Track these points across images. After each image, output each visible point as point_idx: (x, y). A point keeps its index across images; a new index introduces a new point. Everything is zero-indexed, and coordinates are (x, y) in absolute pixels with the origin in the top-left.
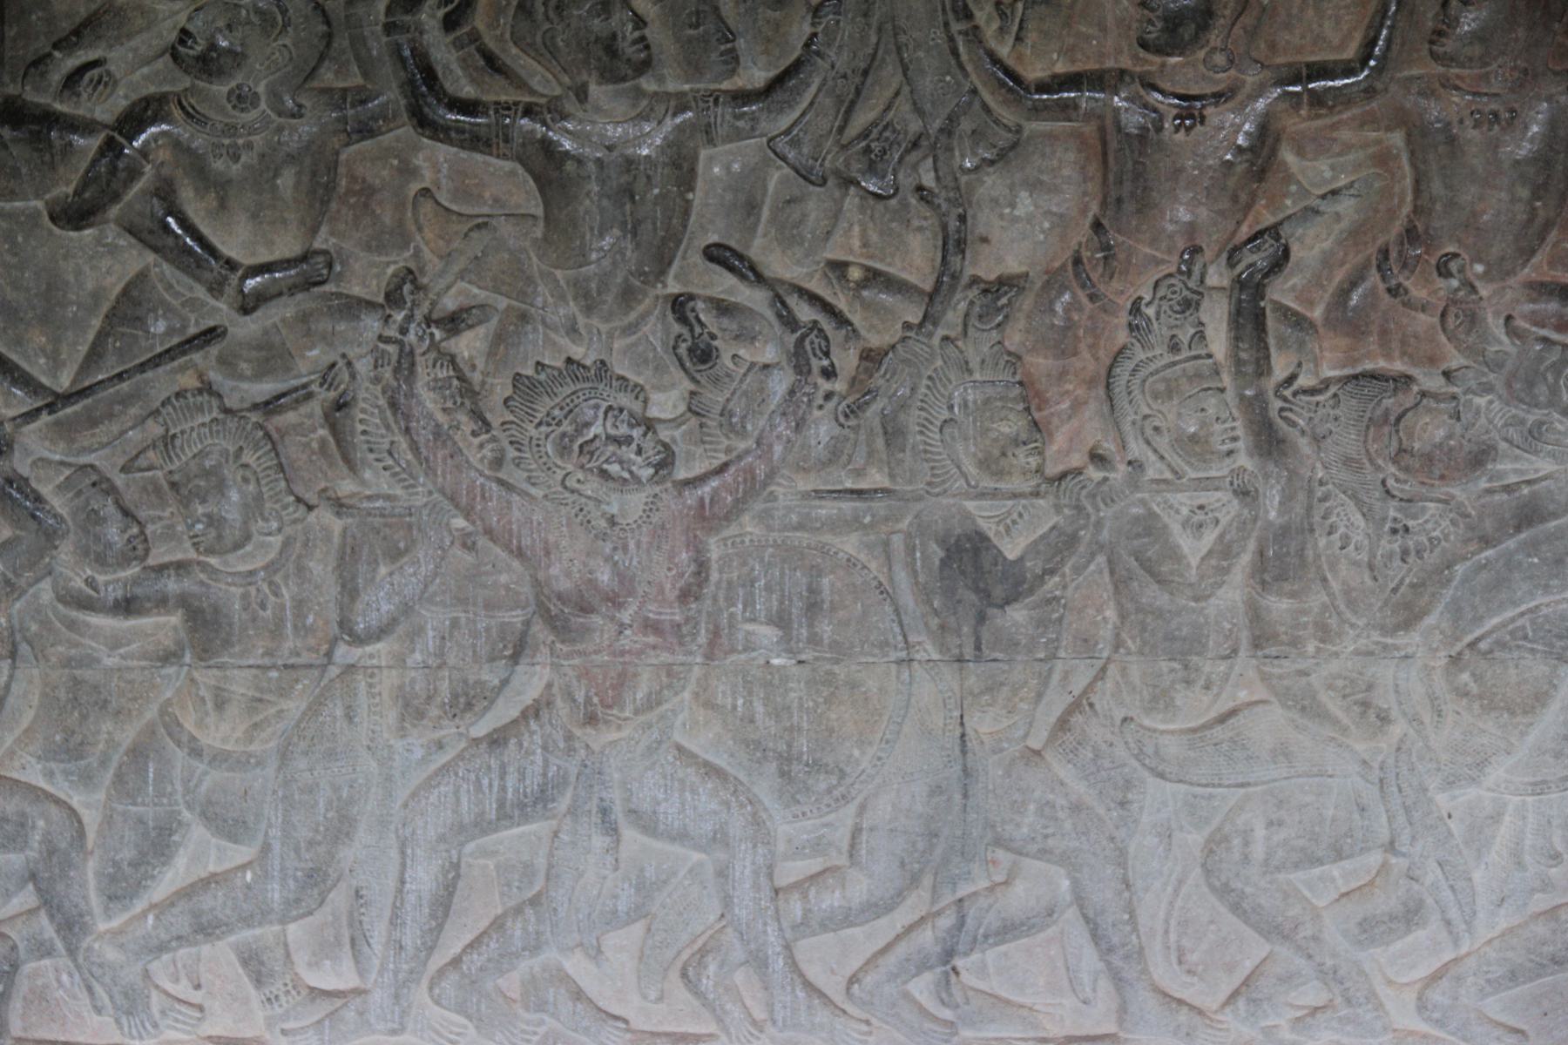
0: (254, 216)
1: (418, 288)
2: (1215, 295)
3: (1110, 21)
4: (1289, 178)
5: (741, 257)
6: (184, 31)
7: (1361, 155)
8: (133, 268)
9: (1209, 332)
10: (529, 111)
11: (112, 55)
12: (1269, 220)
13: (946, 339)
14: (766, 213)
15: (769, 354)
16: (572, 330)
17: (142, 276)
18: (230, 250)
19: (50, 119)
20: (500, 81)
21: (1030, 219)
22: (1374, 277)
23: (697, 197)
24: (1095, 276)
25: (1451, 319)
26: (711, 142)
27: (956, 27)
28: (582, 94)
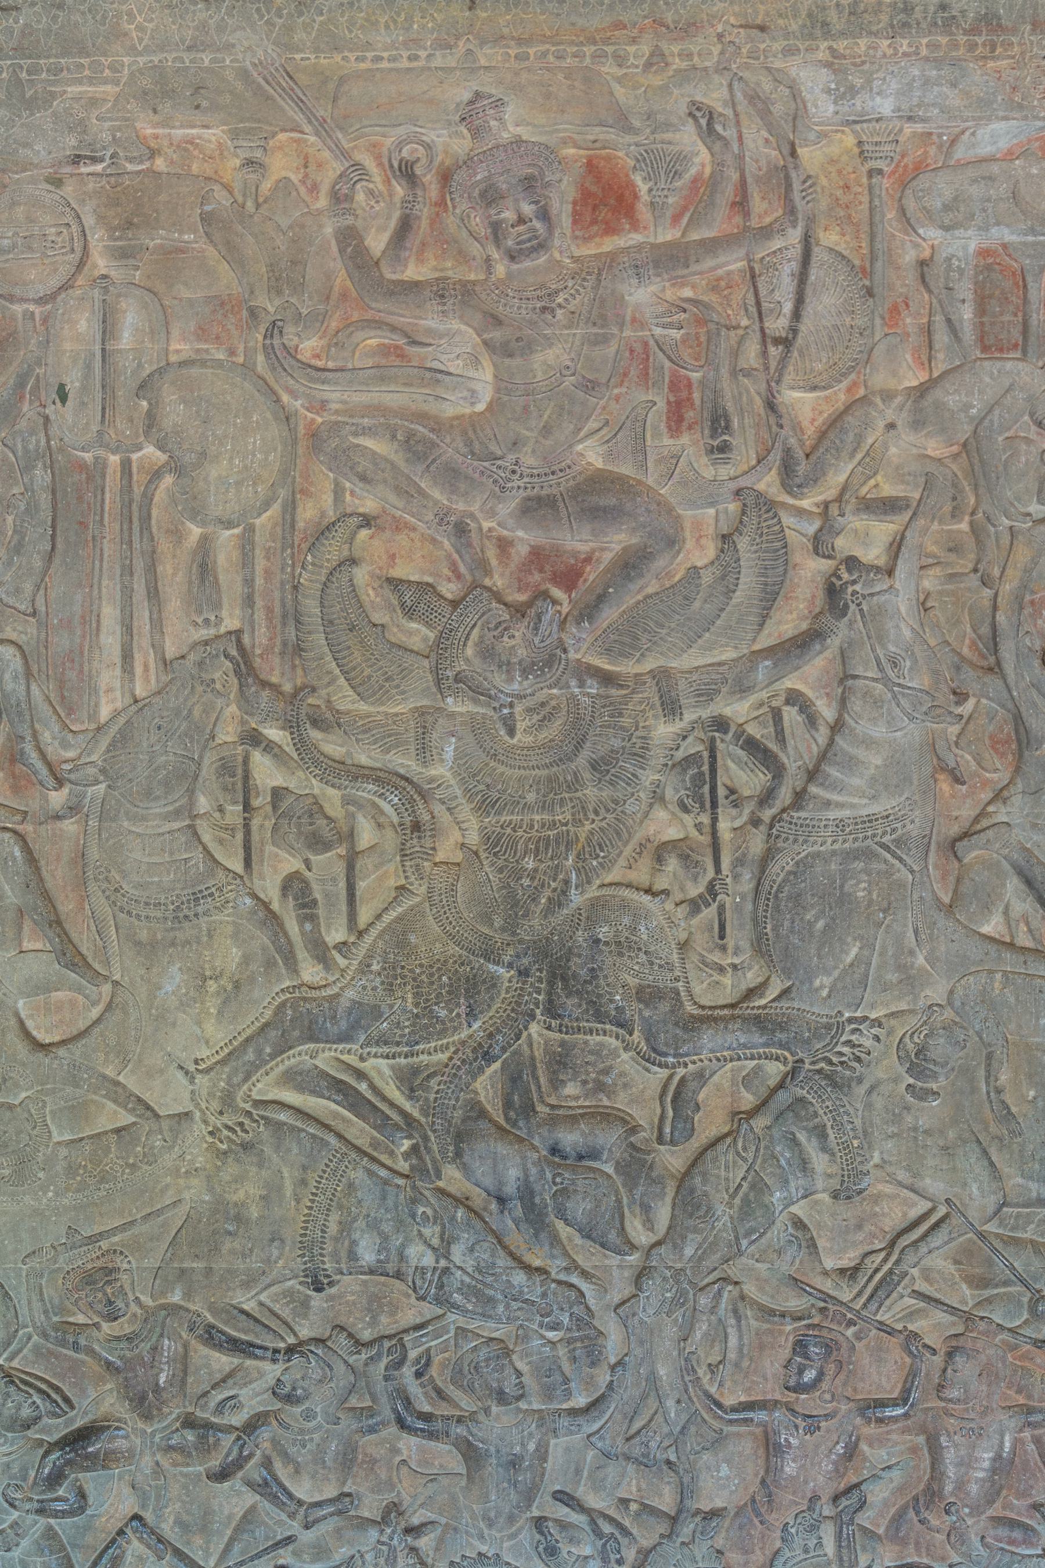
0: (313, 1477)
1: (401, 1514)
2: (828, 1522)
3: (769, 1376)
4: (865, 1459)
5: (573, 1498)
6: (279, 1380)
7: (903, 1447)
8: (249, 1503)
9: (825, 1541)
10: (460, 1420)
11: (243, 1392)
12: (855, 1480)
13: (683, 1543)
14: (585, 1473)
15: (588, 1551)
16: (481, 1537)
17: (253, 1508)
18: (299, 1494)
19: (208, 1426)
20: (444, 1404)
21: (728, 1478)
22: (911, 1514)
23: (548, 1466)
24: (763, 1510)
25: (952, 1538)
26: (556, 1437)
27: (687, 1378)
28: (487, 1411)
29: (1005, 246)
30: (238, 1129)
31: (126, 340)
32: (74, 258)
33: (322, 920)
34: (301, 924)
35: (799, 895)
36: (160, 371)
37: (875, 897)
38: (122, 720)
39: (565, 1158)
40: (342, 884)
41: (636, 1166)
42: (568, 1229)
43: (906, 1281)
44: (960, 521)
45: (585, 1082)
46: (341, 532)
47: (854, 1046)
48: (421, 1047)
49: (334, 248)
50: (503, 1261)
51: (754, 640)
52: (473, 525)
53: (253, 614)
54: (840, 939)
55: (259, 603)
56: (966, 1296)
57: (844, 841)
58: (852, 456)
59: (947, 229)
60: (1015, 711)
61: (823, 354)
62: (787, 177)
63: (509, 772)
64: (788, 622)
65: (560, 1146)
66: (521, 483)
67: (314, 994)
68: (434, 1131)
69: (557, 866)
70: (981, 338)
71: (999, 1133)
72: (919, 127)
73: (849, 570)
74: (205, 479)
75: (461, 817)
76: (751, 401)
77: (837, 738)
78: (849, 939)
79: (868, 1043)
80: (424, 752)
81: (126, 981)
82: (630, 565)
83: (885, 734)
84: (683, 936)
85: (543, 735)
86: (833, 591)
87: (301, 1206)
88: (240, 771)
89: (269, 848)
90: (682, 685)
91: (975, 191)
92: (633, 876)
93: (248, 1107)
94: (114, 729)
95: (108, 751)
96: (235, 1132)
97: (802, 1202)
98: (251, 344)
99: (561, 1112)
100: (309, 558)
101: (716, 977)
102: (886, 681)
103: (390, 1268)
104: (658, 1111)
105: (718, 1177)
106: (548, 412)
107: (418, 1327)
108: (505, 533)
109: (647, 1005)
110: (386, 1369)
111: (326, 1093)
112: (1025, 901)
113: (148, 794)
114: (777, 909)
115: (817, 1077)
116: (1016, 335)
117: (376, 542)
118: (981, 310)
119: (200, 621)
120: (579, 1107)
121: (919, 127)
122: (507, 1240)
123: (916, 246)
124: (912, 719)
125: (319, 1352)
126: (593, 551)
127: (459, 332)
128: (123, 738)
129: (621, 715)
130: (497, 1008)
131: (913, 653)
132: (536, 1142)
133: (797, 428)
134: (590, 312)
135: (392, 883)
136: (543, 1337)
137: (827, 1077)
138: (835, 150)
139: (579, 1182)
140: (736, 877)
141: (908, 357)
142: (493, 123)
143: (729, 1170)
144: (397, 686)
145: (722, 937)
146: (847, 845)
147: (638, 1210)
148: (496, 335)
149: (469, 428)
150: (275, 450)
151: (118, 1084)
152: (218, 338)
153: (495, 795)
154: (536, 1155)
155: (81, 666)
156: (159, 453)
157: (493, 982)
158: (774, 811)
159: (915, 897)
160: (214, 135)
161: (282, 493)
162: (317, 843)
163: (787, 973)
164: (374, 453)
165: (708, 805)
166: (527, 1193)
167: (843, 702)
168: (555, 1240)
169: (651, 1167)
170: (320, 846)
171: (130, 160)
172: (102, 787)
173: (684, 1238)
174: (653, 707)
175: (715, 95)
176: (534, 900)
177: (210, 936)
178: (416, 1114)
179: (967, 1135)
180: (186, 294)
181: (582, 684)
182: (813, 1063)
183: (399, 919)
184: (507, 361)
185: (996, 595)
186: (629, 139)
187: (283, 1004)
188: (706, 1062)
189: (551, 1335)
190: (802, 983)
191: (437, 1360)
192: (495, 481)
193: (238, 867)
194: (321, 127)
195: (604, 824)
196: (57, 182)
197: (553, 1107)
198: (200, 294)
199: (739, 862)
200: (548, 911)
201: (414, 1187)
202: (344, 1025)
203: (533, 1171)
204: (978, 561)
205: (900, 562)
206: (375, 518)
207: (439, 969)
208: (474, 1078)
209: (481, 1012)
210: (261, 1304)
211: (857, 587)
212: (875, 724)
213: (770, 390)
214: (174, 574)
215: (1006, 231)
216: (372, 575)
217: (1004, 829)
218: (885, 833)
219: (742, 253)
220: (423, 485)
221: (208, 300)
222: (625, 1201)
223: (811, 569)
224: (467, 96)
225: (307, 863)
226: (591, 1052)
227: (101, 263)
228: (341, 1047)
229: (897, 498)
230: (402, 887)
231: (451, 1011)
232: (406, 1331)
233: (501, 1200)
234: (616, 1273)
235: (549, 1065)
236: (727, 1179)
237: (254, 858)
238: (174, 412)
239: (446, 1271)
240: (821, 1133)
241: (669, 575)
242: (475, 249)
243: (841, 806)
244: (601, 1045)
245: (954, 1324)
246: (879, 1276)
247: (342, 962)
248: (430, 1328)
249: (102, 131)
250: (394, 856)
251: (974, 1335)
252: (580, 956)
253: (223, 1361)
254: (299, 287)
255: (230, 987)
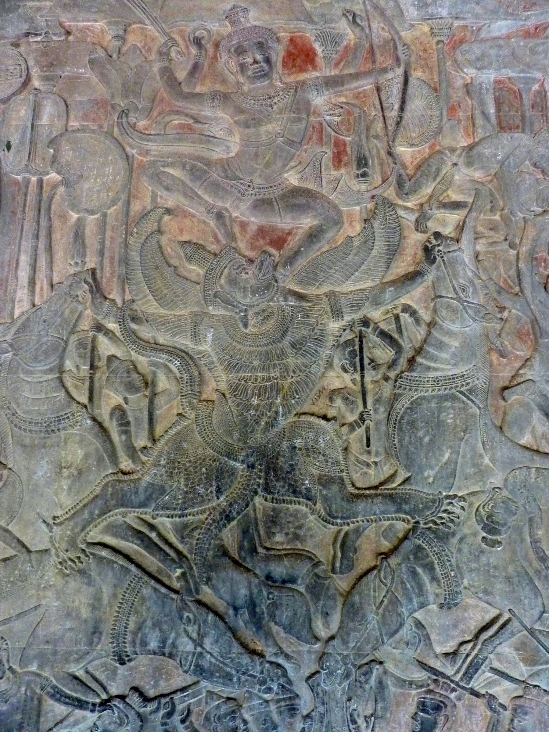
27: (352, 727)
29: (509, 78)
30: (77, 561)
31: (45, 120)
32: (22, 80)
33: (133, 434)
34: (120, 436)
35: (414, 421)
36: (61, 135)
37: (458, 422)
38: (24, 317)
39: (275, 582)
40: (146, 413)
41: (317, 588)
42: (277, 627)
43: (487, 662)
44: (495, 215)
45: (287, 534)
46: (154, 217)
47: (449, 513)
48: (189, 511)
49: (158, 77)
50: (236, 649)
51: (383, 277)
52: (226, 214)
53: (102, 260)
54: (439, 448)
55: (107, 254)
56: (521, 671)
57: (439, 390)
58: (435, 179)
59: (479, 69)
60: (532, 317)
61: (416, 129)
62: (395, 44)
63: (243, 348)
64: (402, 266)
65: (272, 575)
66: (253, 192)
67: (126, 478)
68: (196, 564)
69: (271, 404)
70: (499, 123)
71: (539, 568)
72: (461, 23)
73: (436, 239)
74: (81, 189)
75: (216, 374)
76: (378, 152)
77: (433, 331)
78: (444, 448)
79: (458, 511)
80: (196, 336)
81: (15, 469)
82: (313, 236)
83: (460, 329)
84: (345, 445)
85: (263, 328)
86: (427, 250)
87: (113, 610)
88: (89, 347)
89: (106, 391)
90: (343, 301)
91: (493, 52)
92: (315, 409)
93: (83, 546)
94: (20, 322)
95: (15, 334)
96: (74, 562)
97: (421, 611)
98: (111, 122)
99: (273, 553)
100: (135, 230)
101: (365, 470)
102: (459, 299)
103: (167, 651)
104: (332, 552)
105: (369, 595)
106: (269, 155)
107: (183, 689)
108: (244, 219)
109: (324, 486)
110: (163, 717)
111: (131, 539)
112: (544, 425)
113: (35, 359)
114: (401, 429)
115: (428, 532)
116: (518, 122)
117: (172, 223)
118: (498, 108)
119: (72, 263)
120: (284, 550)
121: (461, 23)
122: (239, 634)
123: (463, 78)
124: (474, 320)
125: (121, 706)
126: (293, 228)
127: (222, 118)
128: (24, 327)
129: (308, 317)
130: (235, 488)
131: (473, 284)
132: (258, 571)
133: (404, 167)
134: (291, 107)
135: (175, 412)
136: (260, 698)
137: (435, 532)
138: (418, 33)
139: (284, 598)
140: (375, 410)
141: (462, 131)
142: (242, 19)
143: (375, 590)
144: (182, 300)
145: (368, 445)
146: (440, 392)
147: (320, 616)
148: (242, 117)
149: (225, 166)
150: (120, 174)
151: (7, 531)
152: (93, 119)
153: (235, 361)
154: (257, 581)
155: (6, 288)
156: (58, 176)
157: (233, 472)
158: (397, 372)
159: (482, 422)
160: (100, 25)
161: (123, 197)
162: (131, 387)
163: (407, 467)
164: (173, 175)
165: (359, 368)
166: (252, 605)
167: (435, 311)
168: (268, 635)
169: (328, 588)
170: (133, 390)
171: (55, 34)
172: (10, 354)
173: (348, 634)
174: (326, 313)
175: (356, 7)
176: (257, 423)
177: (66, 443)
178: (185, 552)
179: (519, 569)
180: (79, 99)
181: (286, 300)
182: (425, 524)
183: (178, 433)
184: (247, 130)
185: (518, 253)
186: (311, 27)
187: (107, 485)
188: (361, 523)
189: (266, 696)
190: (417, 474)
191: (195, 710)
192: (239, 191)
193: (84, 400)
194: (154, 21)
195: (298, 379)
196: (16, 45)
197: (268, 549)
198: (86, 98)
199: (377, 401)
200: (266, 430)
201: (182, 600)
202: (142, 497)
203: (255, 591)
204: (507, 235)
205: (464, 235)
206: (172, 210)
207: (201, 464)
208: (220, 531)
209: (225, 490)
210: (87, 672)
211: (441, 248)
212: (454, 324)
213: (389, 146)
214: (61, 239)
215: (509, 71)
216: (170, 240)
217: (530, 384)
218: (462, 385)
219: (371, 80)
220: (199, 193)
221: (89, 101)
222: (312, 609)
223: (415, 239)
224: (229, 7)
225: (126, 400)
226: (291, 515)
227: (36, 83)
228: (141, 510)
229: (460, 202)
230: (179, 415)
231: (207, 490)
232: (175, 692)
233: (236, 609)
234: (306, 656)
235: (265, 523)
236: (375, 597)
237: (95, 397)
238: (67, 154)
239: (201, 654)
240: (430, 568)
241: (335, 241)
242: (231, 78)
243: (436, 369)
244: (297, 511)
245: (516, 689)
246: (470, 659)
247: (144, 458)
248: (190, 691)
249: (41, 22)
250: (177, 396)
251: (530, 697)
252: (284, 456)
253: (61, 709)
254: (138, 95)
255: (76, 473)
